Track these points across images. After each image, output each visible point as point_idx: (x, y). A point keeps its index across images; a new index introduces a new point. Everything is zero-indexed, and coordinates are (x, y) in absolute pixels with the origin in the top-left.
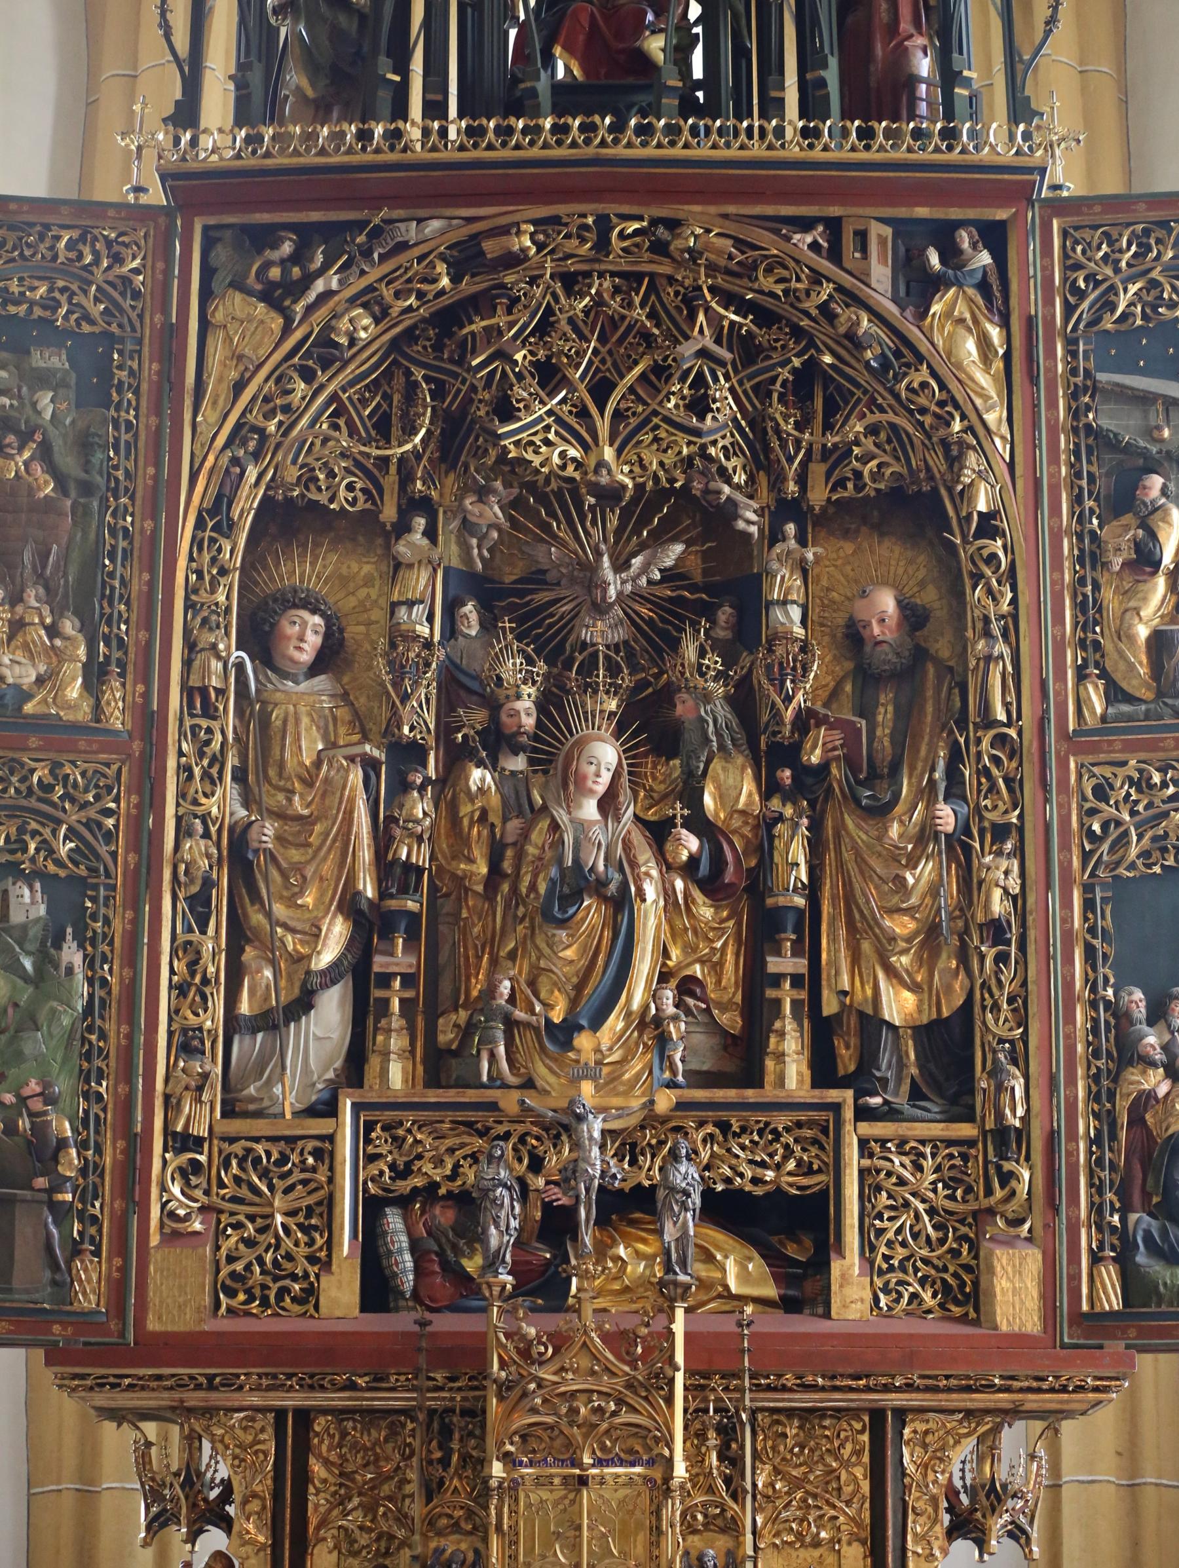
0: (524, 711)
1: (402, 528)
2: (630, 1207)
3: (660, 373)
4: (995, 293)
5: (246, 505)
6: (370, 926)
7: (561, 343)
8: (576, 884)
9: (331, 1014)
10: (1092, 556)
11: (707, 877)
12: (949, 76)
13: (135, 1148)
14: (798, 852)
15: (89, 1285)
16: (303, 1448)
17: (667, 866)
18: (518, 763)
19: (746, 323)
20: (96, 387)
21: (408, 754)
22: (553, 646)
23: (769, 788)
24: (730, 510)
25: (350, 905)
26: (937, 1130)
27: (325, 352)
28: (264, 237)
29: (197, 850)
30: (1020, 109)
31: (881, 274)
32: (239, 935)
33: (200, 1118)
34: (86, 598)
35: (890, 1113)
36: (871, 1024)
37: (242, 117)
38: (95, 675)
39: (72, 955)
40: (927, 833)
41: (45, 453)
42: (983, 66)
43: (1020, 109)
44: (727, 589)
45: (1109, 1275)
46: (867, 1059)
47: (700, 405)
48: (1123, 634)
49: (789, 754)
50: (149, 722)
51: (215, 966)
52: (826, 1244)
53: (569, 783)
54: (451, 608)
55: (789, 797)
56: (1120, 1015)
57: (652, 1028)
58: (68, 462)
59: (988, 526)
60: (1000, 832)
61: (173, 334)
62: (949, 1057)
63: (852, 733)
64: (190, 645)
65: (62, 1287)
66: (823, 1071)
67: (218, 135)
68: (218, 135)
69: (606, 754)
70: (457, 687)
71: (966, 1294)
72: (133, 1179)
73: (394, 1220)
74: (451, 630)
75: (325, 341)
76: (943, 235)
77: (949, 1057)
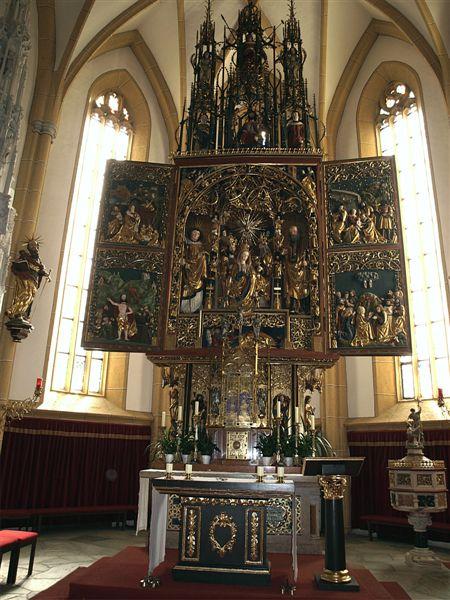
0: (233, 247)
1: (213, 217)
2: (247, 330)
3: (257, 192)
4: (314, 178)
5: (187, 213)
6: (206, 282)
7: (241, 186)
8: (242, 274)
9: (199, 296)
10: (331, 219)
11: (263, 274)
12: (306, 142)
13: (164, 317)
14: (279, 269)
15: (154, 340)
16: (191, 370)
17: (257, 272)
18: (232, 256)
19: (272, 183)
20: (161, 193)
21: (213, 254)
22: (238, 237)
23: (275, 259)
24: (268, 214)
25: (203, 279)
26: (304, 316)
27: (201, 188)
28: (192, 169)
29: (177, 270)
30: (318, 146)
31: (294, 175)
32: (183, 283)
33: (174, 314)
34: (159, 227)
35: (296, 313)
36: (292, 298)
37: (188, 149)
38: (160, 239)
39: (154, 286)
40: (302, 266)
41: (153, 203)
42: (312, 141)
43: (318, 146)
44: (268, 227)
45: (335, 342)
46: (292, 304)
47: (263, 195)
48: (337, 232)
49: (278, 254)
50: (169, 247)
51: (179, 288)
52: (284, 335)
53: (241, 258)
54: (222, 231)
55: (278, 261)
56: (336, 296)
57: (252, 297)
58: (157, 205)
59: (313, 215)
60: (315, 266)
61: (176, 185)
62: (306, 304)
63: (289, 250)
64: (176, 236)
65: (150, 341)
66: (283, 306)
67: (184, 153)
68: (184, 153)
69: (247, 254)
70: (222, 244)
71: (309, 345)
72: (164, 323)
73: (208, 332)
74: (221, 235)
75: (200, 186)
76: (305, 168)
77: (306, 304)
